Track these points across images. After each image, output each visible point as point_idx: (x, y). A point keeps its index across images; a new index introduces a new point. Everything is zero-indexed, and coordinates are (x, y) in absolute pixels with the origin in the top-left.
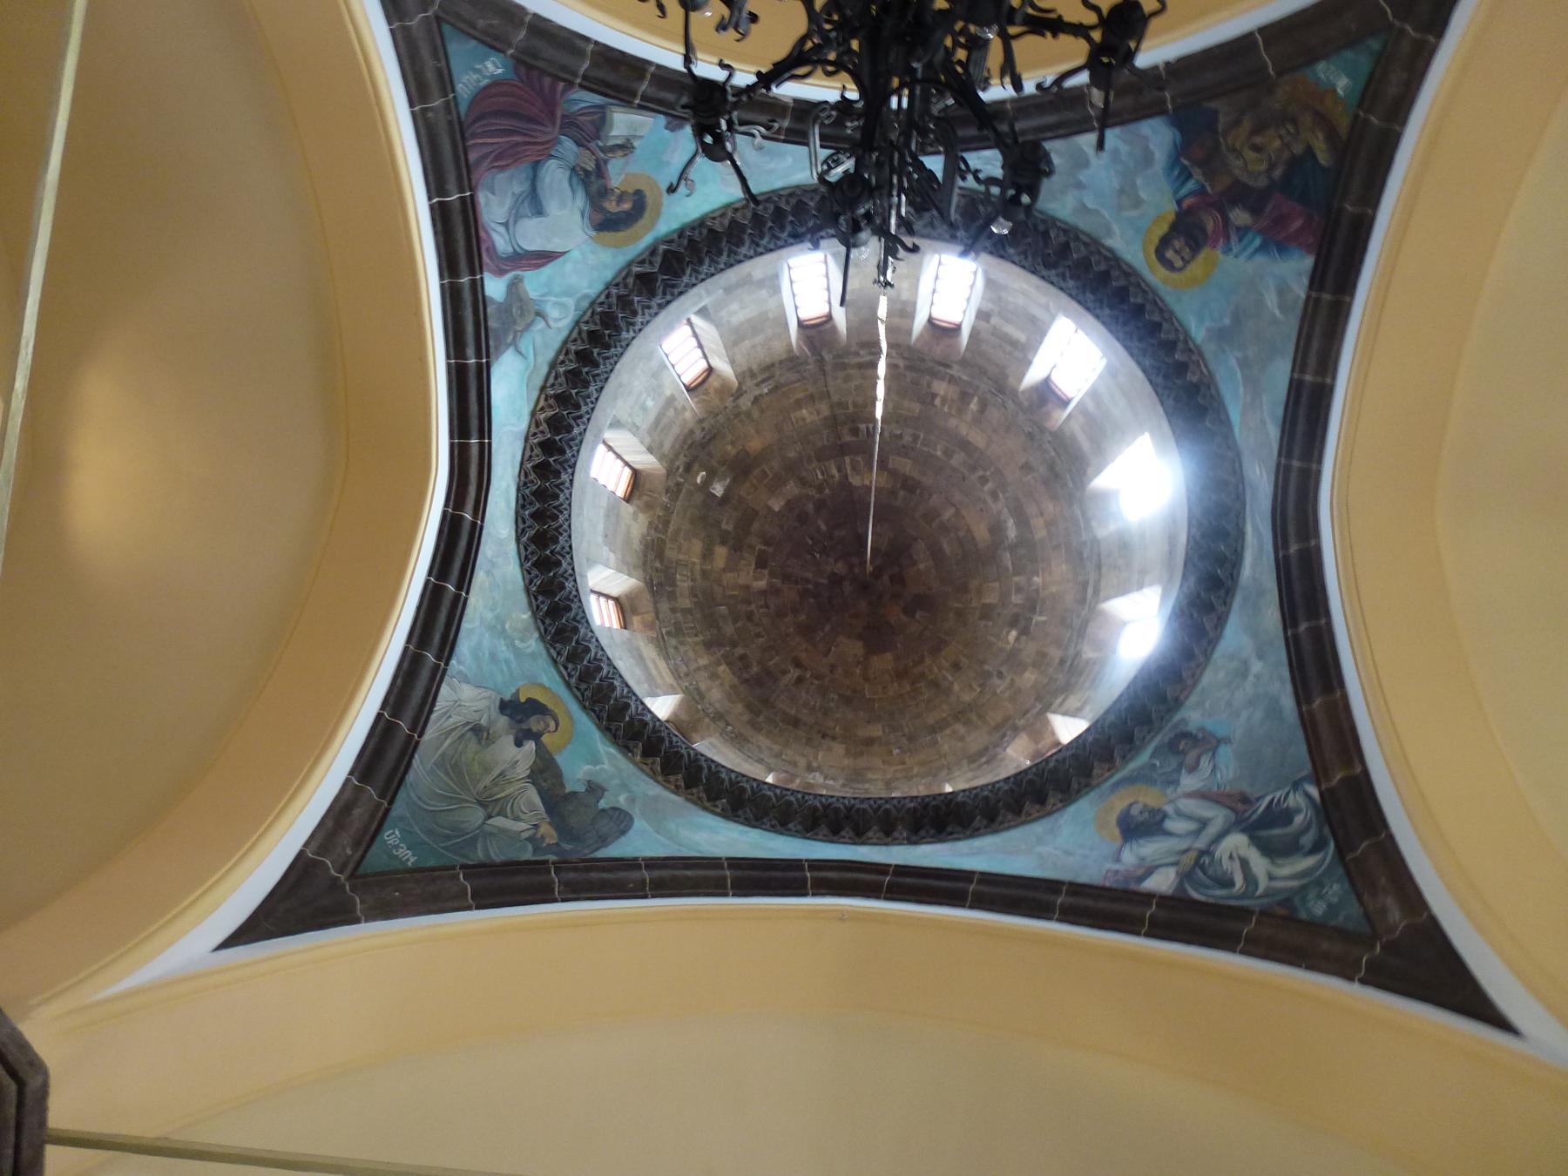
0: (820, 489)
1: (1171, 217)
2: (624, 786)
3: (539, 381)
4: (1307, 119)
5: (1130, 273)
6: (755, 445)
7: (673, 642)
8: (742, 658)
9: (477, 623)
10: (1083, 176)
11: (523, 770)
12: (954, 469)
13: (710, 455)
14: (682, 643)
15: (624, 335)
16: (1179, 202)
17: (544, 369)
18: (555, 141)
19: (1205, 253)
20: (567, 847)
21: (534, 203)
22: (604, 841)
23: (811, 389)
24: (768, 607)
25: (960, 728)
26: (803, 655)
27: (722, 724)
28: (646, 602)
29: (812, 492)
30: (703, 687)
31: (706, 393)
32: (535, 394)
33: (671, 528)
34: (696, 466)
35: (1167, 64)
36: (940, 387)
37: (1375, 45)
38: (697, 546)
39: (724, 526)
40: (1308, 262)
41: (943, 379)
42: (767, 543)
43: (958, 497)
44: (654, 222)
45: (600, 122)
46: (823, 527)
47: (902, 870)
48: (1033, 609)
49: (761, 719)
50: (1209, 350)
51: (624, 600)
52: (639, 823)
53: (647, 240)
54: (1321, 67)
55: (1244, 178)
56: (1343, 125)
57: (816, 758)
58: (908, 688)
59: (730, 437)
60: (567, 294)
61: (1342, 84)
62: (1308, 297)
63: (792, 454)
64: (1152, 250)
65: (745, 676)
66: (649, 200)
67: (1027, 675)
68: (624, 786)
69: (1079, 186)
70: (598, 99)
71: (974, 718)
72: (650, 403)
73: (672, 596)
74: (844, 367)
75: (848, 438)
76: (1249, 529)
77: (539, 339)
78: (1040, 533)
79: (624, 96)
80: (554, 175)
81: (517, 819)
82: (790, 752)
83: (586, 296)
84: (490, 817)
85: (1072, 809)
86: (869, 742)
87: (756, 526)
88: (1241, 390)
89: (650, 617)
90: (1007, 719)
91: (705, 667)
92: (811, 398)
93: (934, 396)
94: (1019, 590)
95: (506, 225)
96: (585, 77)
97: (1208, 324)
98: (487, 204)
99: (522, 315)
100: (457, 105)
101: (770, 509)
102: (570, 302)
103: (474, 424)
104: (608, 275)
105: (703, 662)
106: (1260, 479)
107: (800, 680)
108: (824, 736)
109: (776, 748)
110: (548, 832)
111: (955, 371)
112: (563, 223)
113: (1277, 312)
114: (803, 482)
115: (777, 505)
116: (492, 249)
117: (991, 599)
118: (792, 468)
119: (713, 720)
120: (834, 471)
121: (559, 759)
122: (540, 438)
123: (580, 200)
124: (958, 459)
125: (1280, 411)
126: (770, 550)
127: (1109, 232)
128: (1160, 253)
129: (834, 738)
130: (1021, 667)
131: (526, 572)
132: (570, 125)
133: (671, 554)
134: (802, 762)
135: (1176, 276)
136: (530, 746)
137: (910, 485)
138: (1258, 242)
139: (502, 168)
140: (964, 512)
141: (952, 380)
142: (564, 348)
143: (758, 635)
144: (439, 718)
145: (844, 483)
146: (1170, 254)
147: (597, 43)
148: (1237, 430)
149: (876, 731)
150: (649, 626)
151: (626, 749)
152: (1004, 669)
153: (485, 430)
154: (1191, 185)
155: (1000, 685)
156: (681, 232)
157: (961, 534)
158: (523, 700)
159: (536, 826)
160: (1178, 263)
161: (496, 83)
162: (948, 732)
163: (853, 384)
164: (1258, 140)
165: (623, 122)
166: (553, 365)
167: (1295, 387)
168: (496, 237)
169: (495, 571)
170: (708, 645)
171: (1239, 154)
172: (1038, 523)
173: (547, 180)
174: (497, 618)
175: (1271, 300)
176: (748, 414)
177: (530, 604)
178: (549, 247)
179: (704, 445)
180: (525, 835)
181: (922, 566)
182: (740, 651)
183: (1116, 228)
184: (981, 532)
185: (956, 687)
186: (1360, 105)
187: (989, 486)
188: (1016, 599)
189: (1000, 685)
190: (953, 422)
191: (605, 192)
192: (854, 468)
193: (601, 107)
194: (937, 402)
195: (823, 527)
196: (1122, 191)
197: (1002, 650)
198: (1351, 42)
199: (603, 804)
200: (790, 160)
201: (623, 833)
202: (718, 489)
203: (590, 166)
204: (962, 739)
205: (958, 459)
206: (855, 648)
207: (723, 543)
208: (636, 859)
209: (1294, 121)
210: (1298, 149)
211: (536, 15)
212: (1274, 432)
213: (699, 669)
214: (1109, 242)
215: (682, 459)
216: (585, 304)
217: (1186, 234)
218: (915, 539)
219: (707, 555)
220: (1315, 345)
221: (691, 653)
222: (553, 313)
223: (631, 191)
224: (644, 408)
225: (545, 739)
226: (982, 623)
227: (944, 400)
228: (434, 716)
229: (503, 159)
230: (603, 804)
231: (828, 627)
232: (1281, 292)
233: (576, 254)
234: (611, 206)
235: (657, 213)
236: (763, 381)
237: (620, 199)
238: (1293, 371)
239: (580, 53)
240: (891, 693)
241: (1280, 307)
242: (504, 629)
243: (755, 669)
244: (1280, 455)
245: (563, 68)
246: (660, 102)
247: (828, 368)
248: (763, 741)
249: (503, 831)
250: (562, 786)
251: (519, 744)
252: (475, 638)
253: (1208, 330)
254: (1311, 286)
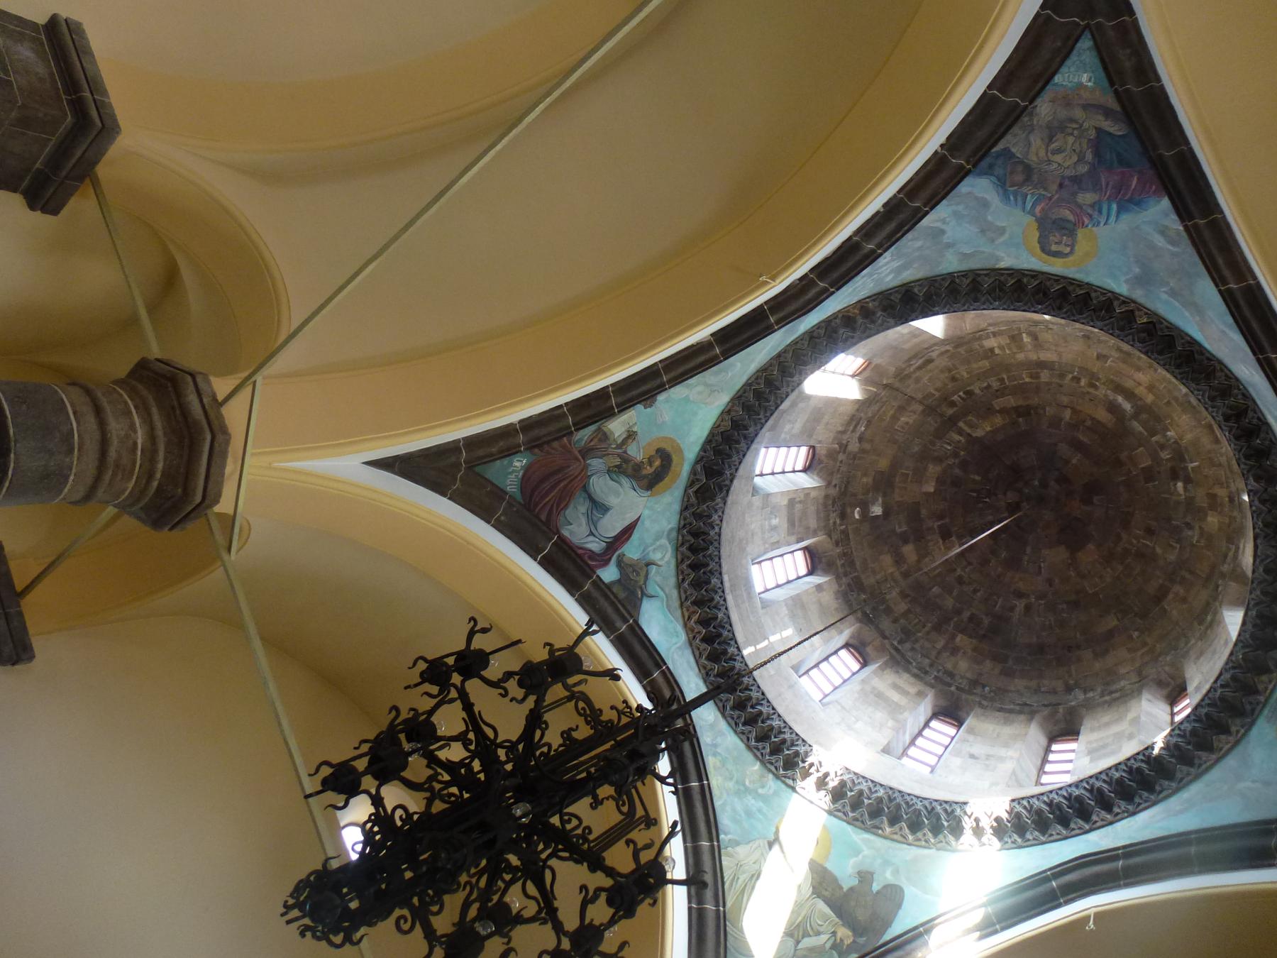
0: (956, 455)
2: (887, 863)
3: (676, 604)
4: (1078, 113)
5: (1035, 274)
6: (883, 464)
7: (908, 645)
8: (971, 619)
9: (725, 796)
10: (946, 239)
12: (1048, 384)
13: (854, 495)
14: (917, 641)
15: (712, 533)
17: (675, 593)
18: (586, 467)
19: (1080, 233)
20: (861, 940)
21: (598, 507)
22: (887, 924)
23: (895, 404)
24: (970, 564)
25: (1178, 589)
26: (1021, 585)
27: (978, 690)
28: (869, 634)
29: (951, 461)
30: (949, 666)
31: (820, 462)
32: (679, 612)
33: (858, 564)
34: (849, 510)
35: (942, 146)
36: (991, 343)
37: (1086, 43)
38: (887, 560)
39: (898, 530)
40: (1165, 203)
41: (988, 337)
42: (941, 517)
43: (1065, 400)
44: (683, 459)
45: (604, 437)
46: (978, 478)
47: (1129, 851)
48: (1182, 459)
49: (1010, 662)
50: (1138, 295)
51: (852, 642)
52: (909, 891)
53: (686, 469)
55: (1068, 173)
56: (1111, 102)
57: (1070, 676)
58: (1120, 568)
59: (859, 474)
60: (658, 538)
61: (1084, 78)
62: (1186, 228)
63: (916, 449)
64: (1038, 250)
65: (982, 632)
66: (669, 449)
67: (1210, 519)
68: (887, 863)
69: (949, 246)
70: (593, 428)
71: (1187, 576)
72: (775, 522)
73: (888, 611)
74: (909, 376)
75: (950, 412)
77: (658, 579)
78: (1150, 398)
79: (609, 414)
80: (600, 485)
81: (818, 933)
82: (1046, 682)
83: (671, 530)
84: (798, 942)
85: (1255, 731)
86: (1110, 634)
87: (924, 512)
88: (1187, 314)
89: (878, 642)
90: (1213, 567)
91: (945, 648)
92: (901, 409)
93: (992, 350)
94: (1162, 447)
95: (592, 534)
96: (574, 425)
97: (1123, 279)
98: (572, 533)
99: (638, 574)
100: (515, 500)
101: (927, 494)
102: (664, 541)
103: (650, 664)
104: (677, 507)
105: (940, 645)
107: (1028, 608)
108: (1069, 649)
109: (1034, 684)
110: (844, 933)
111: (991, 329)
112: (625, 502)
113: (1170, 247)
114: (939, 460)
115: (930, 488)
116: (592, 555)
117: (1146, 463)
118: (925, 457)
119: (970, 692)
120: (957, 437)
122: (699, 637)
123: (625, 482)
124: (1045, 376)
125: (1230, 320)
126: (947, 520)
127: (998, 259)
128: (1045, 249)
129: (1078, 647)
130: (1200, 513)
131: (740, 734)
132: (587, 452)
133: (869, 580)
134: (1059, 685)
135: (1071, 258)
137: (1025, 412)
138: (1114, 206)
139: (566, 506)
140: (1079, 408)
141: (994, 334)
142: (679, 571)
143: (975, 591)
144: (731, 885)
145: (971, 440)
146: (1054, 248)
147: (566, 404)
148: (1206, 345)
149: (1112, 622)
150: (881, 650)
151: (874, 830)
152: (1188, 519)
153: (659, 661)
155: (1194, 535)
156: (703, 449)
157: (1089, 423)
159: (834, 933)
161: (527, 469)
162: (1171, 596)
163: (925, 380)
164: (1053, 146)
165: (617, 427)
166: (679, 586)
167: (1229, 298)
168: (589, 546)
169: (719, 750)
170: (937, 628)
171: (1049, 162)
172: (1141, 391)
173: (598, 490)
174: (737, 782)
175: (1160, 241)
176: (863, 451)
177: (755, 756)
178: (627, 523)
179: (843, 494)
180: (828, 945)
181: (1074, 461)
182: (966, 615)
183: (1001, 254)
184: (1102, 415)
185: (1159, 550)
186: (1112, 83)
187: (1083, 383)
188: (1165, 455)
189: (1194, 535)
190: (1021, 357)
191: (638, 467)
192: (971, 426)
193: (599, 429)
194: (997, 351)
195: (978, 478)
196: (983, 231)
197: (1178, 503)
198: (1064, 54)
199: (876, 887)
200: (739, 365)
201: (899, 906)
202: (877, 510)
203: (617, 461)
204: (1184, 600)
205: (1045, 376)
206: (1057, 555)
207: (906, 542)
209: (1072, 120)
210: (1092, 134)
211: (521, 421)
213: (939, 653)
214: (1002, 265)
215: (834, 517)
216: (674, 534)
217: (1055, 231)
218: (1056, 445)
219: (899, 560)
220: (1220, 261)
221: (927, 645)
222: (656, 556)
223: (653, 453)
224: (774, 528)
226: (1150, 485)
227: (1001, 348)
228: (726, 886)
229: (563, 501)
230: (876, 887)
231: (1028, 550)
232: (1163, 232)
233: (646, 512)
234: (649, 470)
235: (680, 451)
236: (856, 426)
237: (650, 462)
239: (564, 416)
240: (1109, 580)
241: (1172, 243)
242: (747, 789)
243: (986, 621)
245: (560, 430)
246: (630, 400)
247: (897, 385)
248: (1019, 683)
249: (811, 949)
250: (841, 888)
252: (728, 808)
253: (1126, 281)
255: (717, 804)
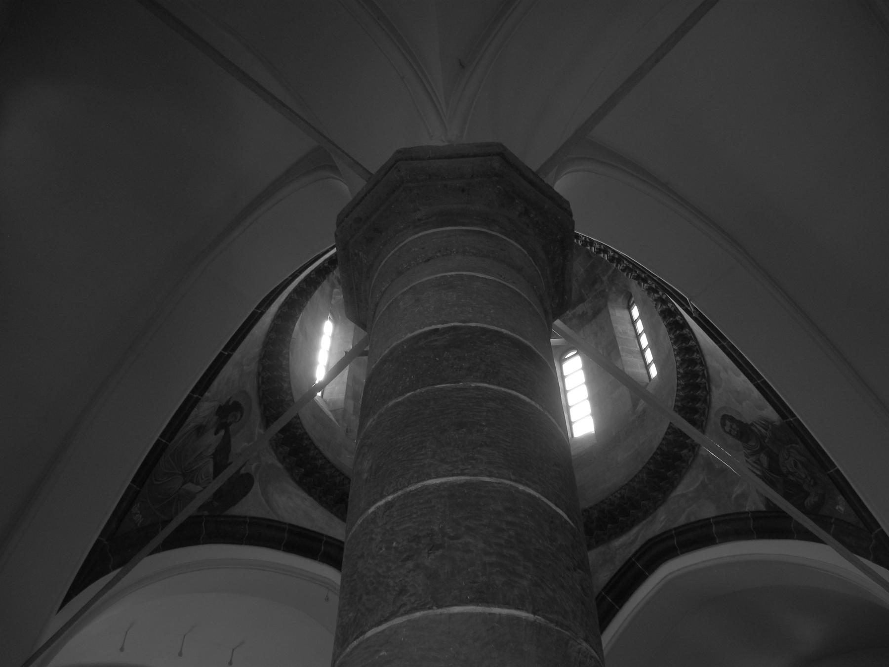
1: (743, 420)
11: (211, 450)
16: (752, 424)
52: (256, 487)
54: (840, 498)
76: (635, 531)
81: (197, 484)
84: (184, 484)
88: (692, 489)
106: (660, 522)
113: (734, 496)
121: (233, 440)
125: (693, 519)
136: (222, 433)
146: (728, 423)
148: (673, 495)
154: (763, 431)
158: (231, 403)
160: (727, 428)
167: (705, 523)
175: (737, 490)
208: (246, 517)
212: (682, 520)
225: (231, 428)
238: (713, 518)
244: (675, 529)
251: (216, 433)
254: (752, 512)
255: (224, 369)
